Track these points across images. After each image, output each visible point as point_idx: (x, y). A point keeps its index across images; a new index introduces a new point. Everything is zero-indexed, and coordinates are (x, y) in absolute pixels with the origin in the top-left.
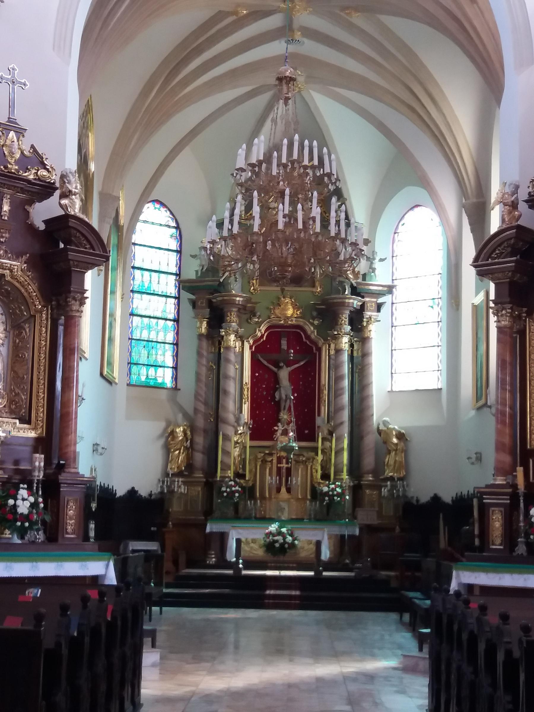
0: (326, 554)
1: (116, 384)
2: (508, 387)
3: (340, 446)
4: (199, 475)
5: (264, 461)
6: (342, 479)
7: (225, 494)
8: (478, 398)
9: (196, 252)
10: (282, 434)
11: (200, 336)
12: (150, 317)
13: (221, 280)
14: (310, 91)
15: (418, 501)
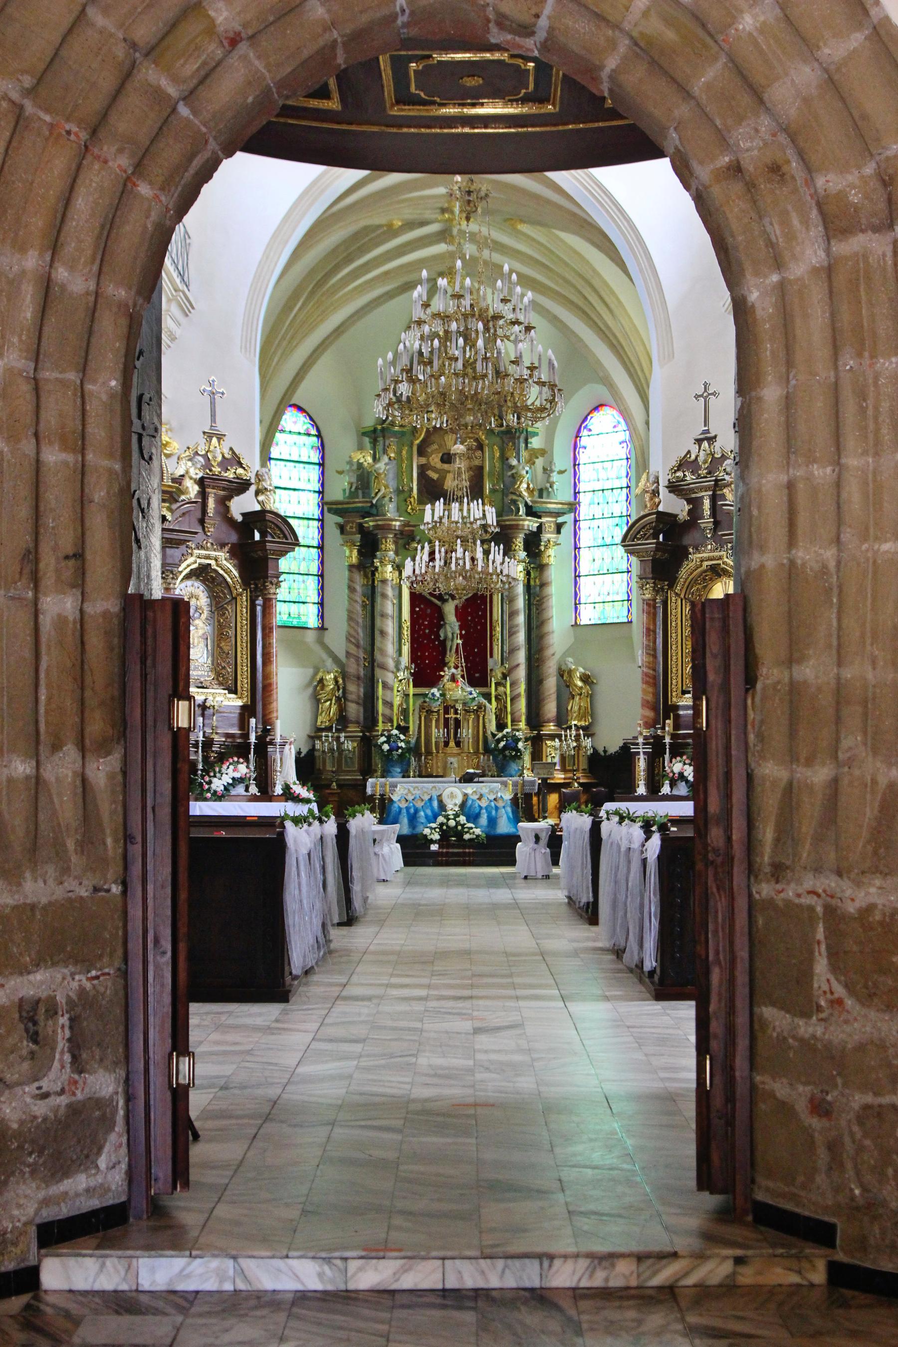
3: (516, 693)
11: (351, 567)
13: (374, 502)
15: (605, 751)
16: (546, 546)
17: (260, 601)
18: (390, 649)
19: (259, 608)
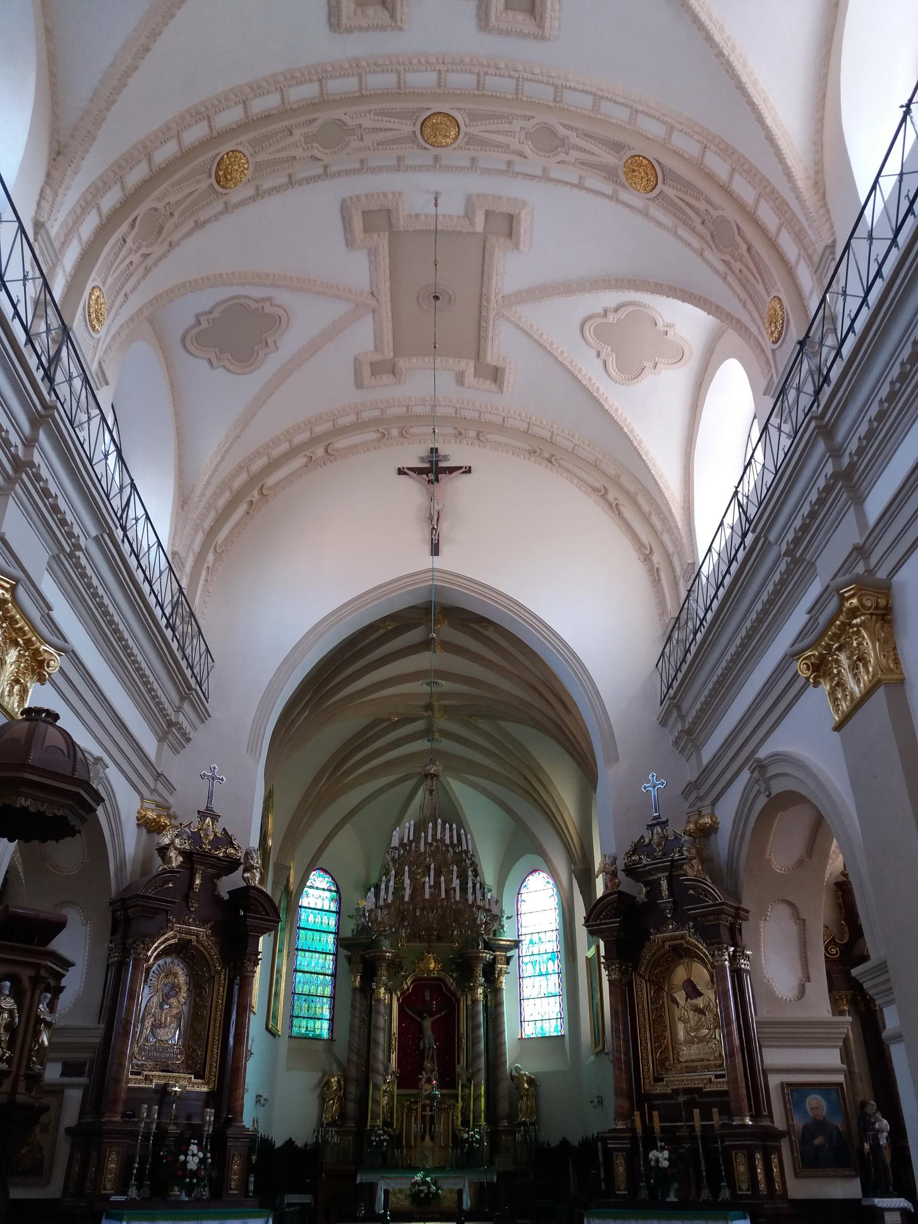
0: (467, 1203)
1: (279, 1036)
2: (622, 1036)
4: (351, 1124)
5: (410, 1110)
6: (481, 1125)
7: (374, 1143)
8: (596, 1044)
9: (354, 913)
10: (426, 1082)
11: (355, 989)
12: (311, 973)
14: (448, 778)
15: (548, 1145)
16: (498, 974)
17: (237, 981)
18: (381, 1055)
19: (236, 988)
